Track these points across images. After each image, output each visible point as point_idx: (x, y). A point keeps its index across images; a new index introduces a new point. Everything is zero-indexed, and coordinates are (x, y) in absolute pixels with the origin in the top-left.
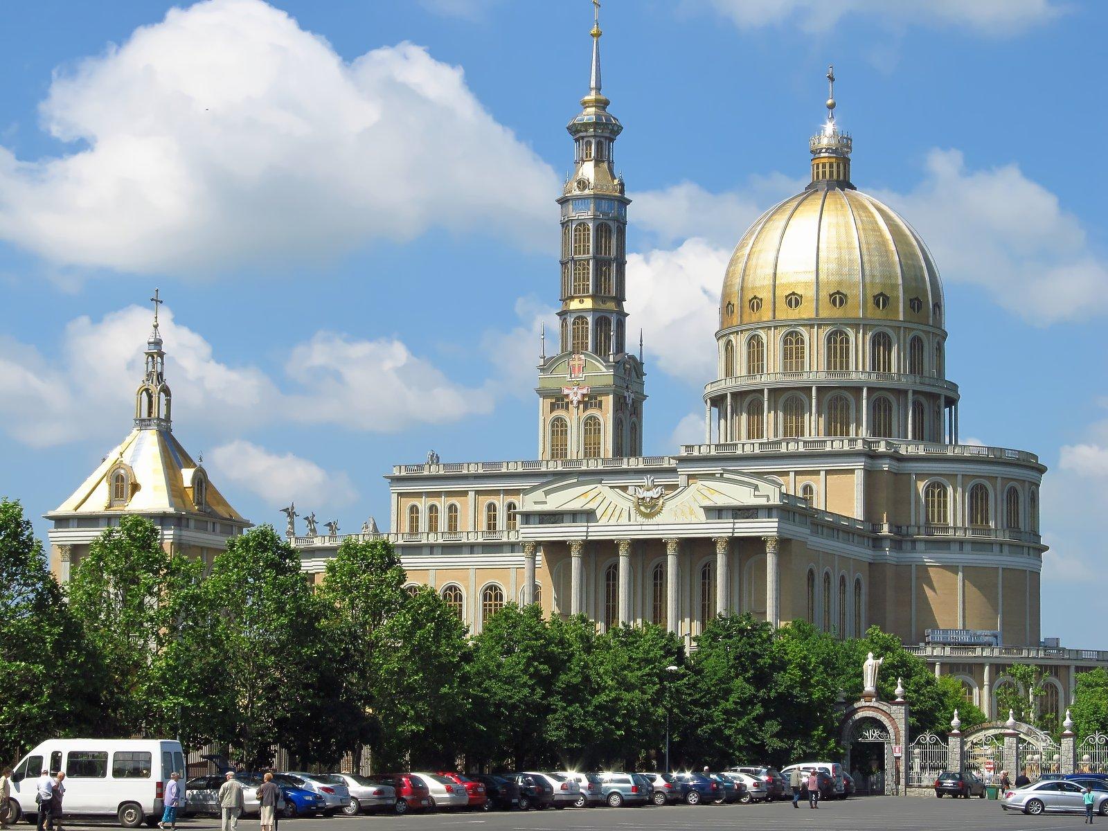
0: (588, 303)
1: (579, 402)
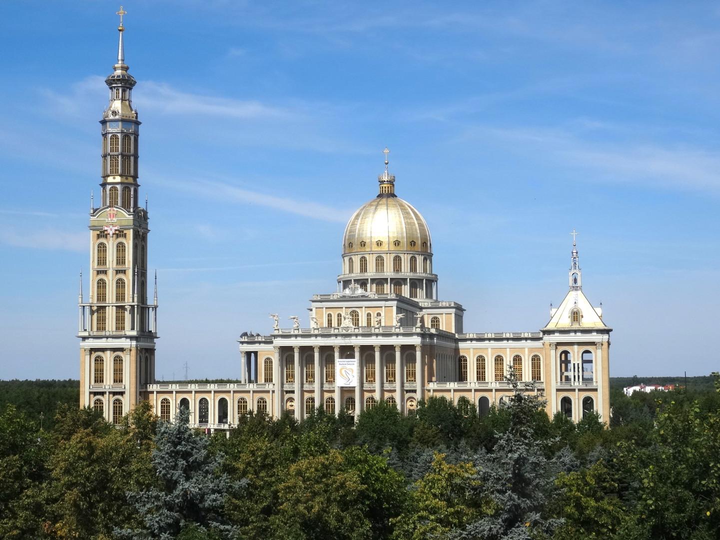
0: (118, 179)
1: (113, 234)
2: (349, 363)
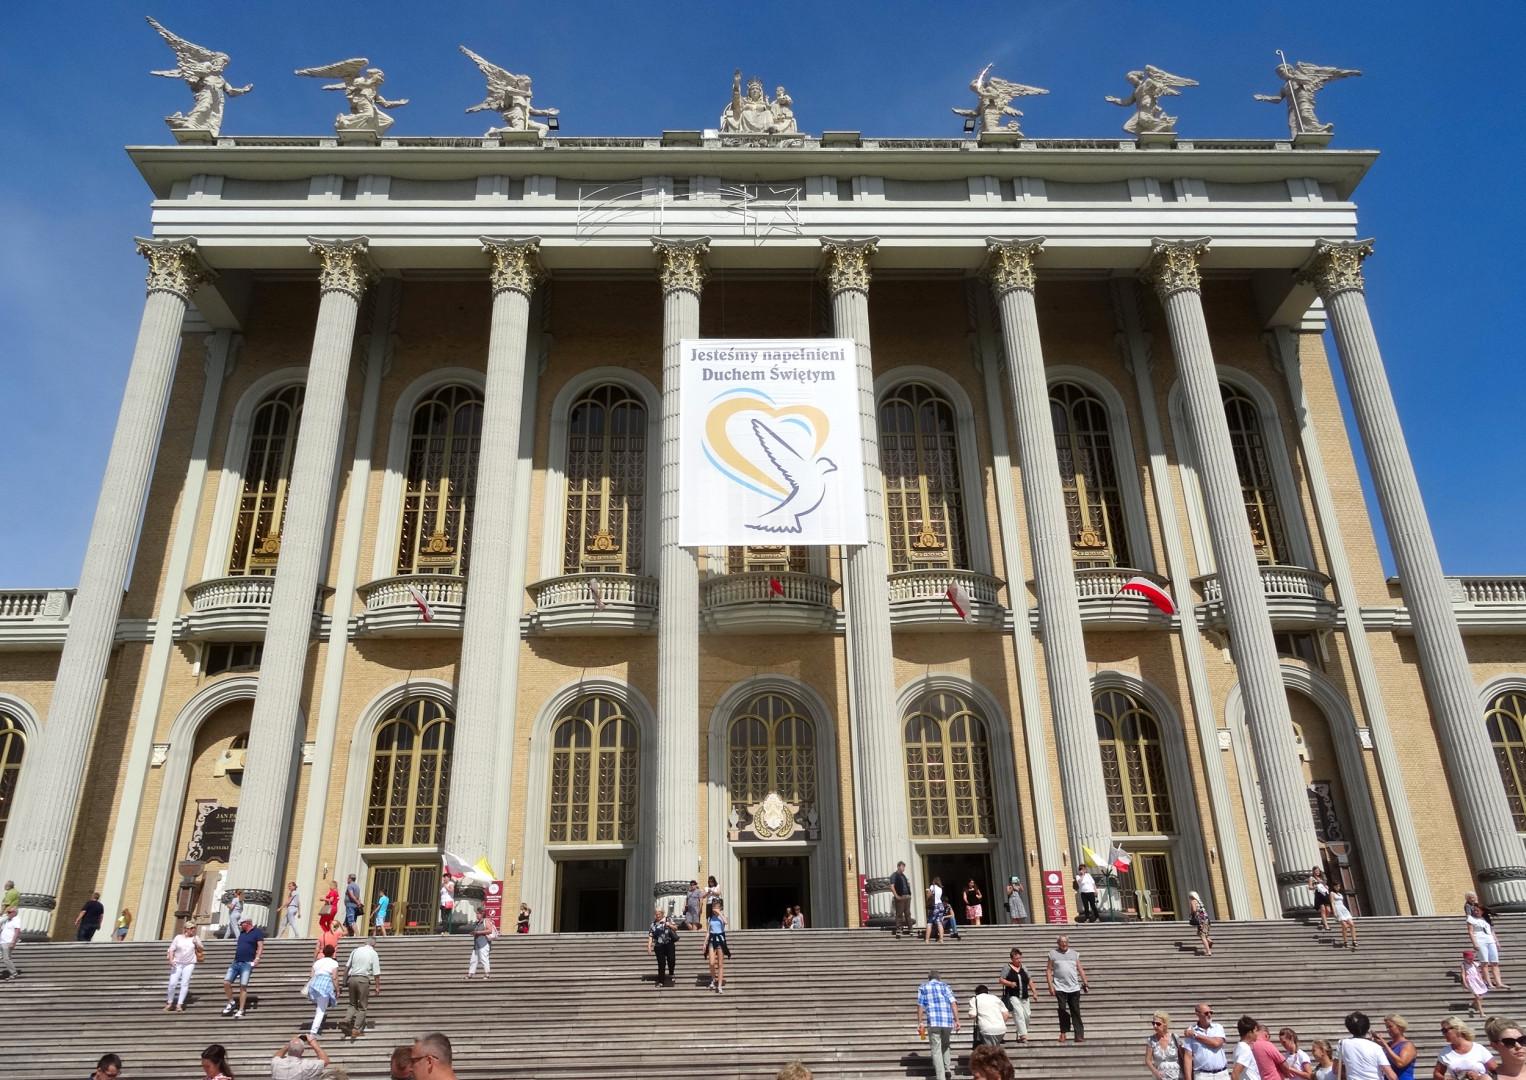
2: (783, 367)
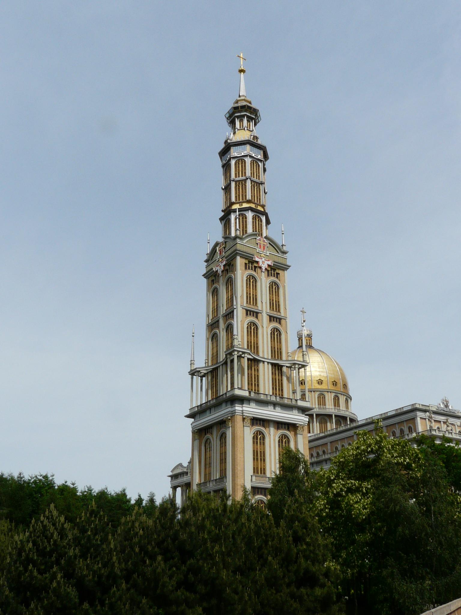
1: (266, 269)
